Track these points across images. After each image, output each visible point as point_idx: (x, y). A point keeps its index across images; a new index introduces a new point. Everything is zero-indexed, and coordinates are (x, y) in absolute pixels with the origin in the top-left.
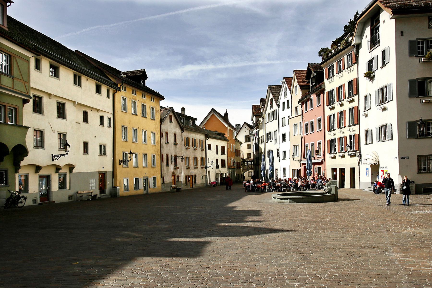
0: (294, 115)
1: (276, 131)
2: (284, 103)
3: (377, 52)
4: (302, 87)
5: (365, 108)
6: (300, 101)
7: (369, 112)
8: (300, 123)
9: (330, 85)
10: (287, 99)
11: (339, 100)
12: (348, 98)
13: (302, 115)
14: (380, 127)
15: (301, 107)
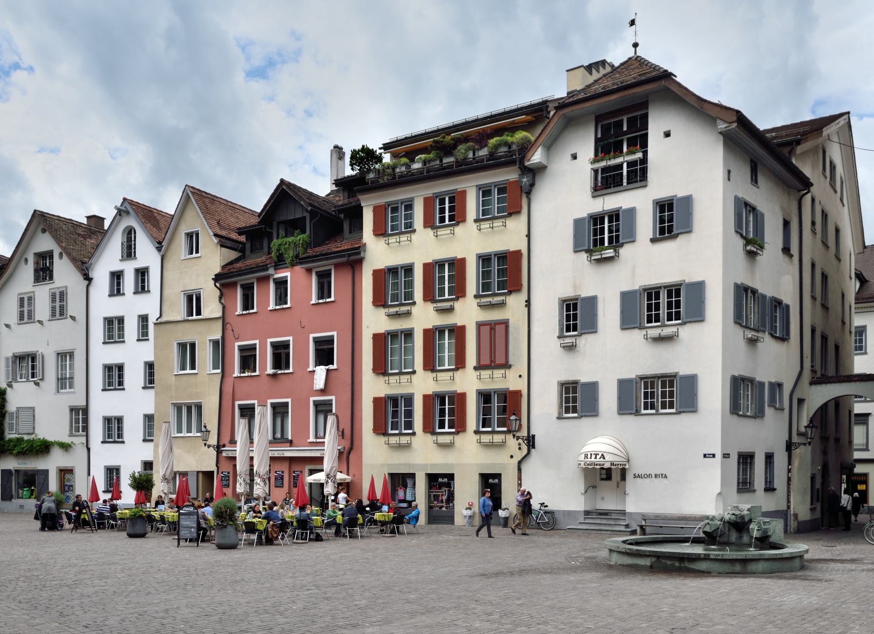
0: (178, 312)
1: (65, 356)
2: (117, 277)
3: (639, 202)
4: (224, 242)
5: (561, 330)
6: (217, 278)
7: (585, 342)
8: (215, 343)
9: (379, 253)
10: (139, 263)
11: (429, 296)
12: (476, 297)
13: (223, 317)
14: (638, 380)
15: (220, 298)
